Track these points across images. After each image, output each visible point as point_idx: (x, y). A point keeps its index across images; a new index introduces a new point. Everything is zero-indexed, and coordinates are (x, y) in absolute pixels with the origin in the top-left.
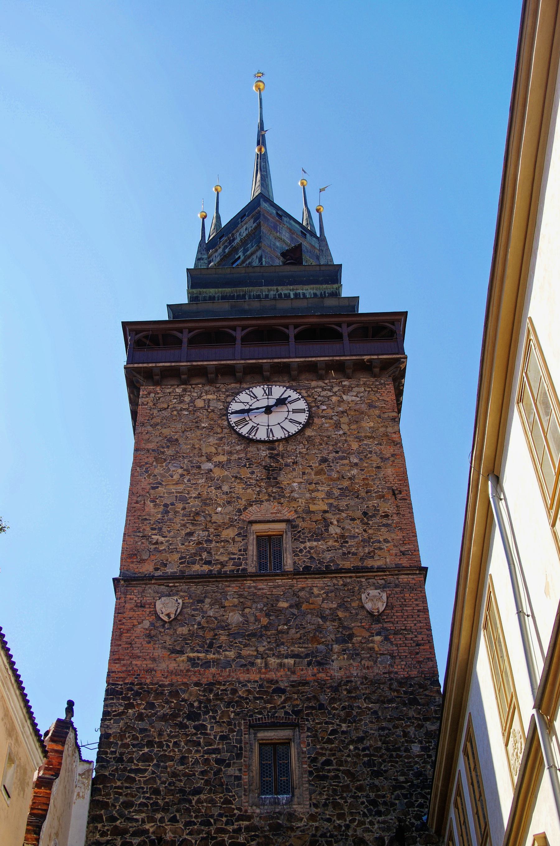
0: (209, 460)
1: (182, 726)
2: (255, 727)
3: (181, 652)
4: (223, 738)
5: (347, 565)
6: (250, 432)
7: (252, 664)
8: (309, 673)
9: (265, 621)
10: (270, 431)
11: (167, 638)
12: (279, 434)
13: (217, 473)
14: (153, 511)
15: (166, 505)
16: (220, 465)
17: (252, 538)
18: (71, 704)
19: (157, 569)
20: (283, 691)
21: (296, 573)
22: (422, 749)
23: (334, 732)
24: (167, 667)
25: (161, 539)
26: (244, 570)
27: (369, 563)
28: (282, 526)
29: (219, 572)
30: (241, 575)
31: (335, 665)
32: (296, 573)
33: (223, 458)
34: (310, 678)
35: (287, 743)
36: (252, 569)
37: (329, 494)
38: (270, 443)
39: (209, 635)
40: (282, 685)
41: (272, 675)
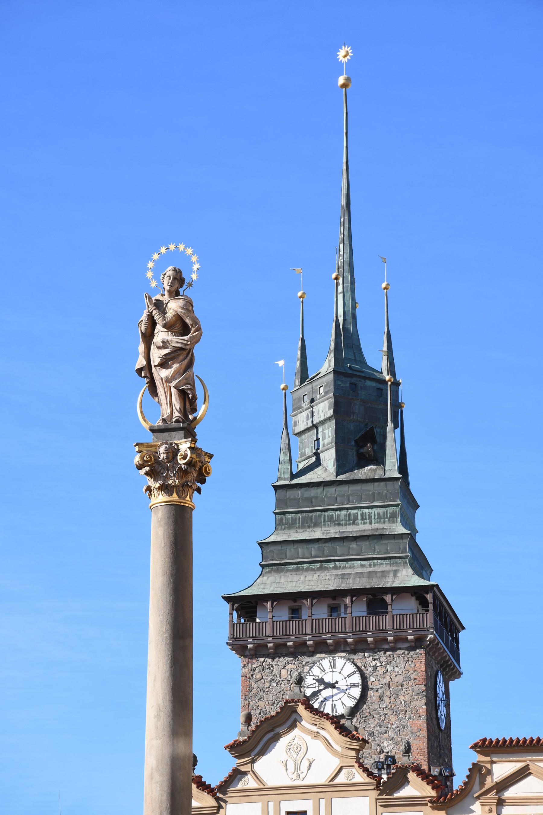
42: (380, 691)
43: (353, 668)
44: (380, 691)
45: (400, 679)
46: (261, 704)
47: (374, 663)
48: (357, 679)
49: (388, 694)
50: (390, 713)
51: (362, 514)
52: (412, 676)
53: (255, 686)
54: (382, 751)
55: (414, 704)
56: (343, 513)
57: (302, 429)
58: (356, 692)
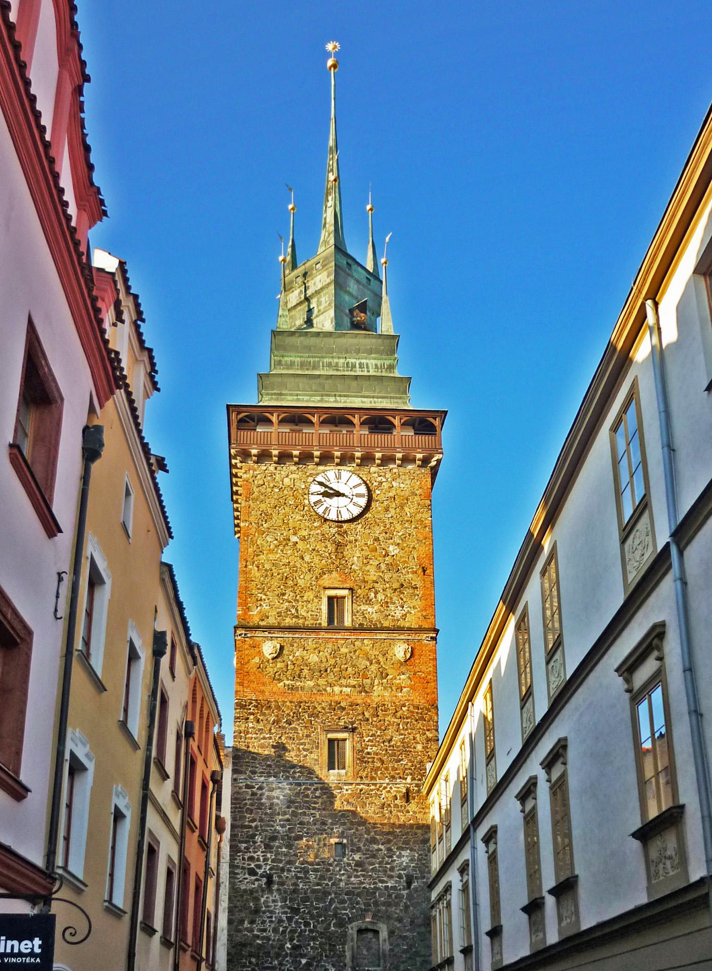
0: (295, 534)
1: (284, 728)
2: (328, 731)
3: (280, 680)
4: (308, 736)
5: (386, 624)
7: (325, 690)
8: (359, 699)
9: (332, 662)
10: (339, 513)
11: (271, 670)
12: (346, 516)
13: (301, 545)
14: (258, 574)
15: (266, 570)
16: (303, 539)
17: (325, 601)
19: (263, 620)
20: (344, 709)
21: (353, 630)
22: (423, 748)
23: (373, 735)
25: (264, 597)
26: (320, 624)
27: (402, 623)
28: (345, 593)
29: (304, 624)
30: (317, 629)
31: (376, 694)
32: (353, 630)
33: (305, 533)
34: (359, 702)
36: (324, 624)
37: (378, 566)
39: (297, 669)
41: (337, 698)
42: (386, 503)
43: (360, 481)
44: (386, 503)
45: (407, 493)
46: (263, 506)
47: (379, 479)
48: (363, 490)
49: (394, 505)
50: (395, 522)
51: (360, 364)
52: (418, 492)
53: (256, 490)
54: (387, 555)
55: (419, 516)
57: (294, 304)
58: (363, 502)
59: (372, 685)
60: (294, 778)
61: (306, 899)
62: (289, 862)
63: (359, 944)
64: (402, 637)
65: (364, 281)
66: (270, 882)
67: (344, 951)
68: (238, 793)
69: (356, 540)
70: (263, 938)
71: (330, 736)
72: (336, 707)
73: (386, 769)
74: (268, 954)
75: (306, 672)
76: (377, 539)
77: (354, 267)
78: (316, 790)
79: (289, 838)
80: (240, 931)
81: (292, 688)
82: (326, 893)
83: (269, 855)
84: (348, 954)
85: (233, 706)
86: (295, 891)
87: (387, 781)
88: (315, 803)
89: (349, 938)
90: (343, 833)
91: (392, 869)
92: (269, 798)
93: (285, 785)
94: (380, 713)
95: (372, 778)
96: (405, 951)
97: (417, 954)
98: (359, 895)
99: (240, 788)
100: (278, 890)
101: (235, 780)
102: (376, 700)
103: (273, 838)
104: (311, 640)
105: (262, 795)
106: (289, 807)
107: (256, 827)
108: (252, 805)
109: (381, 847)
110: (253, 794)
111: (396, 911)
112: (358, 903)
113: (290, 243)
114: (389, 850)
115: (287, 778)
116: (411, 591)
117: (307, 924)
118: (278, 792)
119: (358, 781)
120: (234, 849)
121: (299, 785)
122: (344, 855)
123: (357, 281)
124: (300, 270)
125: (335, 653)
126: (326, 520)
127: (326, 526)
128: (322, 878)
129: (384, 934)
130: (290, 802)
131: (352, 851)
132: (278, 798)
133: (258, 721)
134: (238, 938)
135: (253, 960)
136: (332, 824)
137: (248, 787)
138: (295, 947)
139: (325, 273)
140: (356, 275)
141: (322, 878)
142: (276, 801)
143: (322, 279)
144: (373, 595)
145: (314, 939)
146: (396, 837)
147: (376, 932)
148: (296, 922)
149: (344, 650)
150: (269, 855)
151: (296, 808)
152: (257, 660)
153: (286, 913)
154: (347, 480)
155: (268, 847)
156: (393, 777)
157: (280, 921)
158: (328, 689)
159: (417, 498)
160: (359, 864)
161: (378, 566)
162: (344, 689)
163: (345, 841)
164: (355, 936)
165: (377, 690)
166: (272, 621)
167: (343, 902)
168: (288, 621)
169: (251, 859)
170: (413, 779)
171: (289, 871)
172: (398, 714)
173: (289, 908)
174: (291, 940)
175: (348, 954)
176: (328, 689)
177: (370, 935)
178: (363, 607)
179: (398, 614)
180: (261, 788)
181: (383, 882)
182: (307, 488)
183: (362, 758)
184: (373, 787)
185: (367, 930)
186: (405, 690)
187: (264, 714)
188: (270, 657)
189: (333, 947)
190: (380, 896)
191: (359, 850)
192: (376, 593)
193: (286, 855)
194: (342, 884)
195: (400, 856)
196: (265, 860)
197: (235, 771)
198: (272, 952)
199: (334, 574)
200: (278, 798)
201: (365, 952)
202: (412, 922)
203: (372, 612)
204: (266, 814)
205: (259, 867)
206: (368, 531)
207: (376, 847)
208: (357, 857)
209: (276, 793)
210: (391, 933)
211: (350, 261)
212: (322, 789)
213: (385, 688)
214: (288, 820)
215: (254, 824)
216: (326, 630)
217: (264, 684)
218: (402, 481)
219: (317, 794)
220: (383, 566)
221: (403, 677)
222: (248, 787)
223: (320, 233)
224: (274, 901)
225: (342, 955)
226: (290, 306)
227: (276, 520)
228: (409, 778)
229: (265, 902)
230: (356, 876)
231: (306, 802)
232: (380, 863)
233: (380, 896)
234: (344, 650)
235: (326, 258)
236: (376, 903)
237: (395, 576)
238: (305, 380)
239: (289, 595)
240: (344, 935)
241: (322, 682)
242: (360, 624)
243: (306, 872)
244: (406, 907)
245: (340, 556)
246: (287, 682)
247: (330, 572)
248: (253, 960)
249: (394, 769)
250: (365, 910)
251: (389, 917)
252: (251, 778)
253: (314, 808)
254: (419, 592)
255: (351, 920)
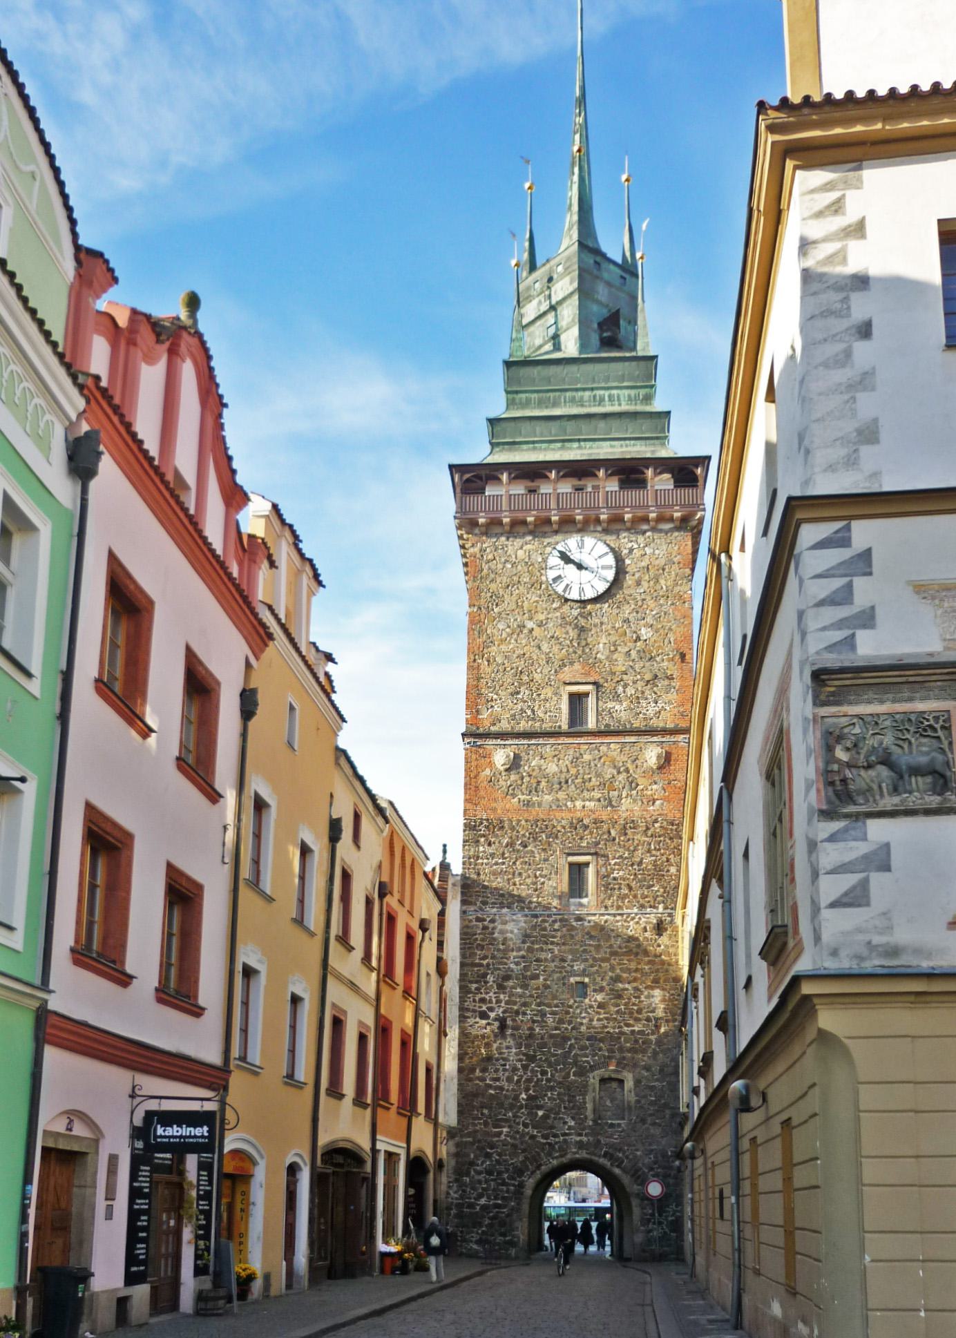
0: (531, 619)
2: (569, 854)
3: (514, 796)
4: (546, 860)
6: (565, 591)
9: (573, 771)
10: (582, 590)
12: (590, 594)
15: (498, 665)
17: (565, 698)
18: (445, 846)
20: (586, 827)
23: (621, 857)
24: (508, 806)
33: (542, 617)
34: (604, 818)
35: (587, 864)
36: (565, 727)
37: (628, 653)
38: (583, 603)
39: (534, 781)
40: (586, 821)
41: (579, 815)
42: (637, 575)
43: (607, 549)
44: (637, 575)
45: (662, 562)
46: (493, 586)
47: (630, 545)
48: (610, 560)
49: (647, 577)
50: (648, 598)
51: (610, 396)
52: (676, 560)
53: (485, 567)
54: (638, 639)
55: (677, 589)
56: (587, 394)
57: (532, 318)
58: (610, 575)
59: (620, 797)
60: (529, 908)
61: (544, 1045)
62: (525, 1004)
63: (603, 1094)
64: (655, 739)
65: (618, 282)
66: (503, 1027)
67: (585, 1103)
68: (467, 927)
69: (602, 623)
70: (496, 1088)
71: (571, 859)
72: (577, 825)
73: (635, 896)
74: (501, 1105)
75: (543, 784)
76: (627, 621)
77: (605, 265)
78: (554, 922)
79: (525, 977)
80: (470, 1080)
81: (528, 804)
82: (565, 1039)
83: (502, 996)
84: (589, 1106)
85: (462, 828)
86: (531, 1036)
87: (635, 910)
88: (554, 937)
89: (590, 1089)
90: (584, 970)
91: (639, 1011)
92: (502, 932)
93: (519, 917)
94: (629, 832)
95: (619, 908)
96: (652, 1103)
97: (666, 1106)
98: (601, 1040)
99: (470, 921)
100: (512, 1035)
101: (464, 912)
102: (624, 815)
103: (507, 978)
104: (548, 747)
105: (494, 928)
106: (524, 942)
107: (488, 965)
108: (483, 940)
109: (627, 986)
110: (485, 928)
111: (643, 1059)
112: (600, 1049)
113: (528, 236)
114: (636, 989)
115: (522, 908)
116: (666, 682)
117: (544, 1073)
118: (512, 926)
119: (603, 911)
120: (464, 991)
121: (536, 916)
122: (585, 995)
123: (609, 284)
124: (540, 273)
125: (576, 760)
126: (567, 600)
127: (566, 608)
128: (561, 1021)
129: (629, 1084)
130: (526, 937)
131: (595, 991)
132: (512, 932)
133: (490, 844)
134: (470, 1088)
135: (486, 1111)
136: (573, 961)
137: (478, 919)
138: (530, 1098)
139: (567, 279)
140: (606, 275)
141: (561, 1021)
142: (509, 935)
143: (565, 286)
144: (620, 689)
145: (552, 1089)
146: (644, 974)
147: (621, 1082)
148: (532, 1071)
149: (587, 757)
150: (502, 996)
151: (533, 943)
152: (488, 772)
153: (520, 1060)
154: (592, 550)
155: (501, 987)
156: (642, 906)
157: (515, 1069)
158: (569, 803)
159: (675, 567)
160: (601, 1006)
161: (628, 653)
162: (587, 803)
163: (587, 980)
164: (597, 1086)
165: (626, 803)
166: (504, 726)
167: (583, 1048)
168: (523, 726)
169: (483, 1000)
170: (666, 908)
171: (524, 1014)
172: (649, 833)
173: (524, 1054)
174: (527, 1090)
175: (589, 1106)
176: (569, 803)
177: (614, 1085)
178: (610, 705)
179: (651, 710)
180: (493, 921)
181: (628, 1025)
182: (545, 560)
183: (607, 884)
184: (618, 918)
185: (611, 1079)
186: (658, 802)
187: (497, 836)
188: (502, 768)
189: (572, 1098)
190: (626, 1041)
191: (602, 989)
192: (625, 686)
193: (520, 996)
194: (583, 1029)
195: (648, 997)
196: (498, 1001)
197: (464, 902)
198: (507, 1103)
199: (577, 666)
200: (512, 932)
201: (608, 1103)
202: (661, 1071)
203: (621, 711)
204: (499, 950)
205: (491, 1009)
206: (615, 611)
207: (620, 985)
208: (599, 997)
209: (509, 927)
210: (637, 1082)
211: (598, 259)
212: (561, 920)
213: (635, 801)
214: (523, 957)
215: (485, 962)
216: (567, 734)
217: (495, 800)
218: (652, 550)
219: (556, 926)
220: (633, 653)
221: (655, 787)
222: (478, 919)
223: (565, 217)
224: (508, 1047)
225: (583, 1106)
226: (525, 322)
227: (509, 602)
228: (661, 907)
229: (498, 1048)
230: (599, 1020)
231: (544, 936)
232: (625, 1004)
233: (626, 1041)
234: (587, 757)
235: (568, 259)
236: (621, 1049)
237: (648, 664)
238: (543, 424)
239: (524, 693)
240: (585, 1086)
241: (561, 795)
242: (607, 725)
243: (543, 1015)
244: (655, 1053)
245: (583, 643)
246: (522, 797)
247: (572, 663)
248: (486, 1111)
249: (644, 897)
250: (609, 1057)
251: (635, 1065)
252: (481, 909)
253: (552, 943)
254: (676, 683)
255: (593, 1068)
